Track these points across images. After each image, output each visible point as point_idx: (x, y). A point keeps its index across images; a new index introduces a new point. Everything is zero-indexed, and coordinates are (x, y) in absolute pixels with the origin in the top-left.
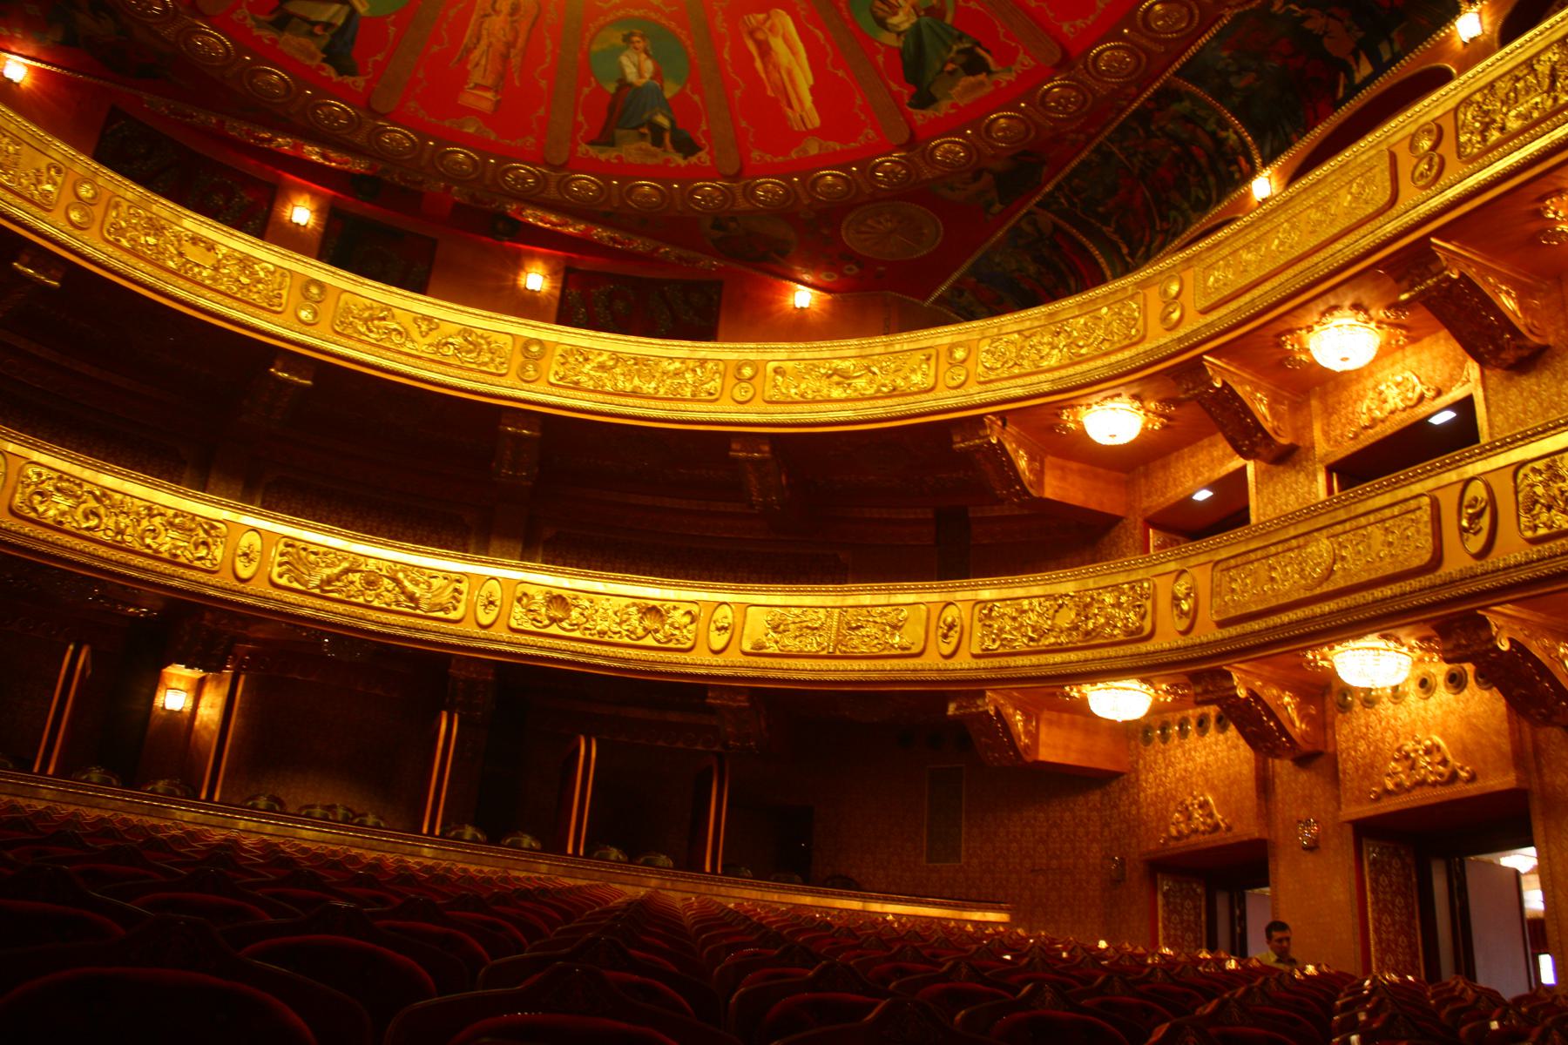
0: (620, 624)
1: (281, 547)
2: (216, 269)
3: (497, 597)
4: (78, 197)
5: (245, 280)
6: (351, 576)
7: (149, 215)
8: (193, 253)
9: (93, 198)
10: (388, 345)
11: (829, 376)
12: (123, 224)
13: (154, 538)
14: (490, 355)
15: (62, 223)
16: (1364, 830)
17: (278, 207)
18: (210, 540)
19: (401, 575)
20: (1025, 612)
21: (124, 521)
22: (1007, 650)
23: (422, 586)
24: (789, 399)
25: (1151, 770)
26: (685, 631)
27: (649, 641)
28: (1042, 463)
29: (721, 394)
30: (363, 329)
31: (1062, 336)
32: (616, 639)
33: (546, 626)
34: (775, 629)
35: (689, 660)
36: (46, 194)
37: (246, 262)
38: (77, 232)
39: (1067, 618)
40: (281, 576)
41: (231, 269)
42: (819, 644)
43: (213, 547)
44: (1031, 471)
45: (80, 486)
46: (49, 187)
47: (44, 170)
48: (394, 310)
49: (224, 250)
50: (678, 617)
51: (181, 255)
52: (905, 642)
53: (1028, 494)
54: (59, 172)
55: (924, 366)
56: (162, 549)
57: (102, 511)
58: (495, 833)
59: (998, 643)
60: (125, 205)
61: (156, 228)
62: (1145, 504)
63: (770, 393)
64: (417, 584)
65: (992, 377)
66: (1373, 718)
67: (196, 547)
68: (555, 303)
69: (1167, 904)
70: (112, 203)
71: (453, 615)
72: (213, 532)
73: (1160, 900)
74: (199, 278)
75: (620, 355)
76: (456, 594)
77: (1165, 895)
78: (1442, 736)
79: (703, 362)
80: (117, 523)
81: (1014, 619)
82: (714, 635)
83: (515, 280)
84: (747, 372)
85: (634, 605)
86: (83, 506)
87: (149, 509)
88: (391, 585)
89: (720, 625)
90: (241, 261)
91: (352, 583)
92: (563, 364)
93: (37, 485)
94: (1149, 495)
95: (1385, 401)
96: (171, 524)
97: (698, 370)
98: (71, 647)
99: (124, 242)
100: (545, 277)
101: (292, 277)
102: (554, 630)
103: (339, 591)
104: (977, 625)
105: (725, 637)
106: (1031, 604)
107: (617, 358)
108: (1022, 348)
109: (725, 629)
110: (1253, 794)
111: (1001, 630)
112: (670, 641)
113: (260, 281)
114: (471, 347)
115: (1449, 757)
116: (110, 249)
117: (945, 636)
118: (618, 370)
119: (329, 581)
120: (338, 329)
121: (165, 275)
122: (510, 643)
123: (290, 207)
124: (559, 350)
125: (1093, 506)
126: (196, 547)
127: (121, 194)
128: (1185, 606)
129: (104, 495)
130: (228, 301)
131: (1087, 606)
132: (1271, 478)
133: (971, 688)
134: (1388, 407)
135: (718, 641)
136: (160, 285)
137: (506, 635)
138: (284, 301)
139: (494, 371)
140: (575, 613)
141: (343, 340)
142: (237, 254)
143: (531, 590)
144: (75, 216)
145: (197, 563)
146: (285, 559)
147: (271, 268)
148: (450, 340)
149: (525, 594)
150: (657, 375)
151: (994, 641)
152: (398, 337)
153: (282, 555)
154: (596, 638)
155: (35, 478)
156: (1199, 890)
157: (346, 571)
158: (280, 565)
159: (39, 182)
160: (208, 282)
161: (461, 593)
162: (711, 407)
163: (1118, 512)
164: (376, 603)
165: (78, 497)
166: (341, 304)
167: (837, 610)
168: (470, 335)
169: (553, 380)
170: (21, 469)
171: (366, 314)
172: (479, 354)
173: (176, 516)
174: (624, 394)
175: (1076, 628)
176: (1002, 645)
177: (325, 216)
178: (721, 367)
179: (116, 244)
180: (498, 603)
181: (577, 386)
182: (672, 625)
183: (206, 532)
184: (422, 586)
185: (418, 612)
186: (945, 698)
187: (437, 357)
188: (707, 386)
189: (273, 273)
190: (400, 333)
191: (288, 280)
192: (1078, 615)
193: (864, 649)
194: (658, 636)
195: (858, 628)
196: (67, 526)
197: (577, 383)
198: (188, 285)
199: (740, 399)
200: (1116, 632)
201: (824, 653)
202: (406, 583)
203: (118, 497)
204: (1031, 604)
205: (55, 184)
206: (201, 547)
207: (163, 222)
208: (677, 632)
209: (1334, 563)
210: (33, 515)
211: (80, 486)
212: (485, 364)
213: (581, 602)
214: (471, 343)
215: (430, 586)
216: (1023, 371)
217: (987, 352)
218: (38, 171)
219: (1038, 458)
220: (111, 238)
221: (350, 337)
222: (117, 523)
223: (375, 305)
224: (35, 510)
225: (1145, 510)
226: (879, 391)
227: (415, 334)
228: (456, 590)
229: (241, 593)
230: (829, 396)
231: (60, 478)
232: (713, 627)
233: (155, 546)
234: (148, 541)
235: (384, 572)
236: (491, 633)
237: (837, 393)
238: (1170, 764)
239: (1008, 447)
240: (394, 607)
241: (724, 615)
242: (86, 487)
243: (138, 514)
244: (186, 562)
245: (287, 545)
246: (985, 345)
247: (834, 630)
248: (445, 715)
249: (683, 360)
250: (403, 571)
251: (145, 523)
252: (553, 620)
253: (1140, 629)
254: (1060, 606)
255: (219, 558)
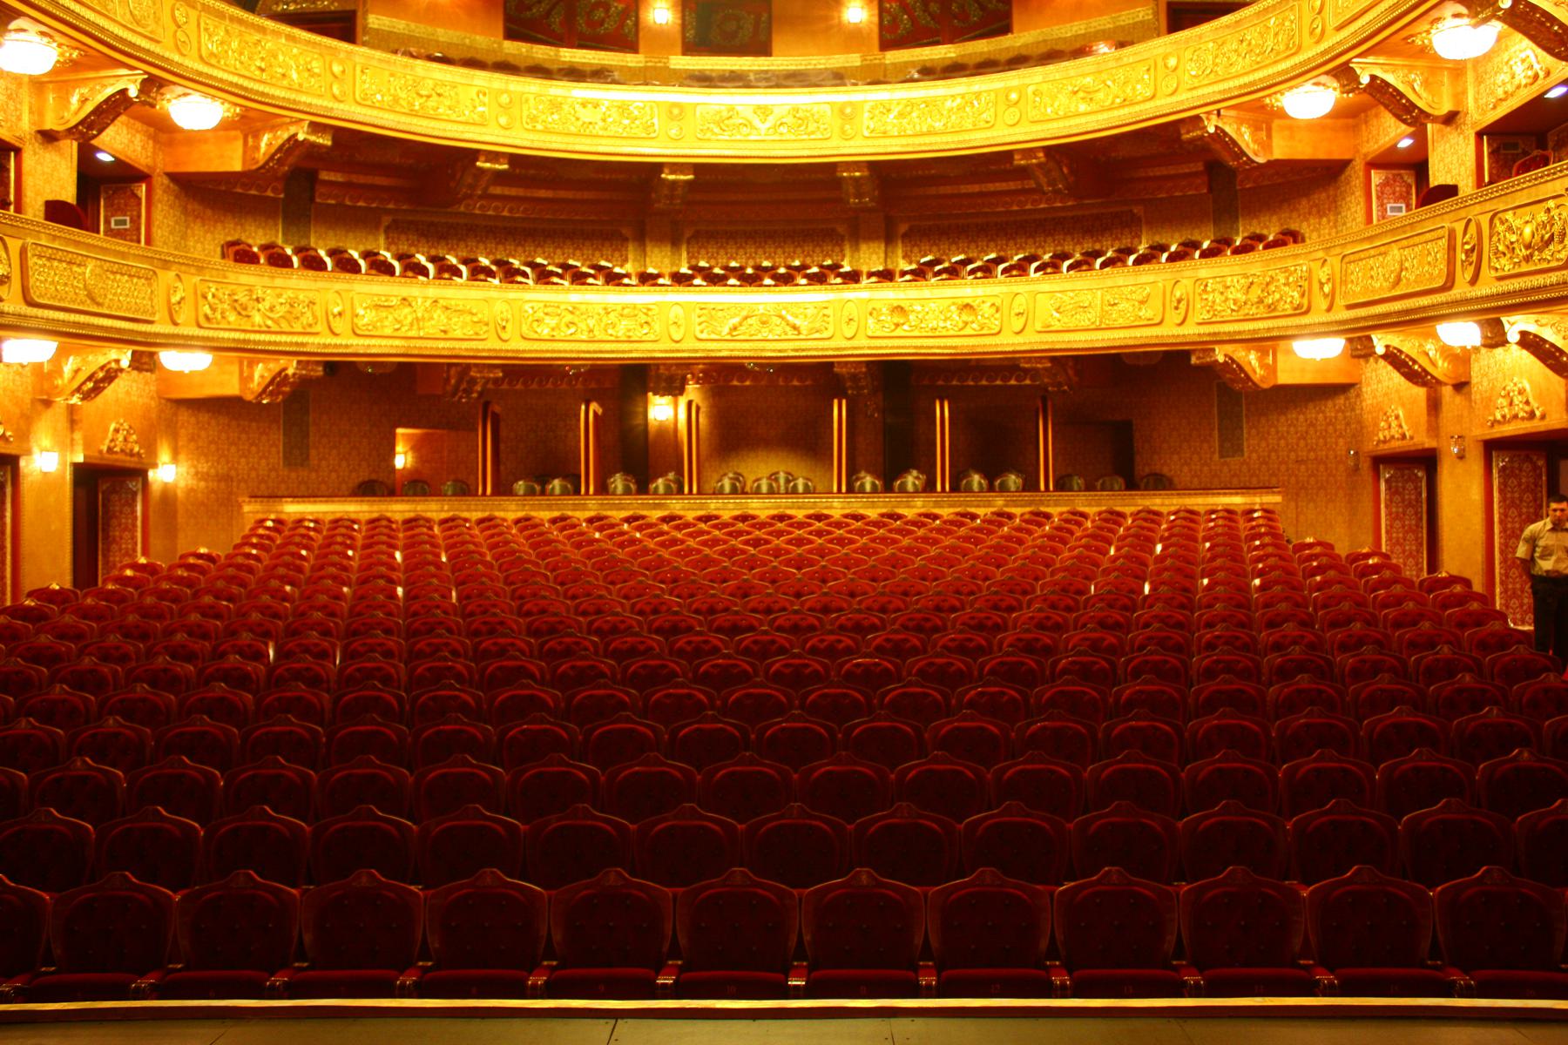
0: (945, 320)
1: (698, 312)
2: (604, 120)
3: (855, 315)
4: (500, 106)
5: (626, 122)
6: (750, 321)
7: (549, 98)
8: (587, 115)
9: (511, 102)
10: (738, 137)
11: (1075, 93)
12: (535, 112)
13: (614, 328)
14: (815, 125)
15: (498, 131)
16: (1492, 447)
17: (642, 15)
18: (649, 319)
19: (784, 313)
20: (1229, 287)
21: (591, 322)
22: (1218, 319)
23: (800, 316)
24: (1047, 118)
25: (1368, 385)
26: (992, 319)
27: (968, 331)
28: (1269, 131)
29: (995, 120)
30: (717, 130)
31: (1244, 44)
32: (944, 333)
33: (893, 331)
34: (1057, 310)
35: (998, 342)
36: (482, 115)
37: (623, 108)
38: (507, 133)
39: (1256, 292)
40: (702, 332)
41: (615, 114)
42: (1089, 320)
43: (652, 324)
44: (1255, 141)
45: (558, 307)
46: (480, 109)
47: (476, 98)
48: (737, 108)
49: (607, 104)
50: (987, 310)
51: (578, 119)
52: (1149, 314)
53: (1253, 161)
54: (485, 94)
55: (1146, 77)
56: (619, 334)
57: (576, 320)
58: (889, 481)
59: (1212, 313)
60: (531, 97)
61: (556, 106)
62: (1364, 150)
63: (1033, 114)
64: (797, 317)
65: (1196, 85)
66: (1492, 361)
67: (642, 327)
68: (876, 29)
69: (1389, 488)
70: (523, 100)
71: (826, 334)
72: (650, 313)
73: (1383, 486)
74: (594, 132)
75: (914, 101)
76: (825, 318)
77: (1387, 481)
78: (1531, 382)
79: (978, 95)
80: (587, 325)
81: (1222, 293)
82: (1014, 319)
83: (839, 17)
84: (1014, 96)
85: (954, 304)
86: (564, 320)
87: (605, 309)
88: (778, 321)
89: (1017, 311)
90: (620, 107)
91: (751, 325)
92: (872, 118)
93: (532, 315)
94: (1368, 142)
95: (1513, 77)
96: (622, 315)
97: (975, 102)
98: (583, 407)
99: (539, 127)
100: (862, 8)
101: (658, 107)
102: (899, 332)
103: (744, 334)
104: (1198, 298)
105: (1022, 320)
106: (1232, 280)
107: (911, 104)
108: (1216, 57)
109: (1022, 314)
110: (1425, 411)
111: (1214, 302)
112: (982, 329)
113: (636, 119)
114: (800, 122)
115: (1531, 400)
116: (531, 136)
117: (1176, 308)
118: (915, 114)
119: (735, 328)
120: (699, 136)
121: (571, 139)
122: (869, 348)
123: (651, 11)
124: (867, 107)
125: (1321, 155)
126: (642, 327)
127: (527, 90)
128: (1327, 289)
129: (574, 308)
130: (618, 142)
131: (1268, 284)
132: (1443, 136)
133: (1207, 346)
134: (1516, 82)
135: (1018, 324)
136: (570, 148)
137: (866, 342)
138: (656, 127)
139: (820, 137)
140: (912, 317)
141: (706, 144)
142: (615, 104)
143: (877, 306)
144: (503, 120)
145: (644, 338)
146: (702, 319)
147: (642, 105)
148: (784, 120)
149: (874, 309)
150: (945, 112)
151: (1208, 312)
152: (745, 129)
153: (699, 317)
154: (930, 334)
155: (531, 311)
156: (1420, 474)
157: (746, 318)
158: (700, 324)
159: (475, 107)
160: (601, 133)
161: (829, 317)
162: (989, 134)
163: (1346, 157)
164: (770, 337)
165: (559, 315)
166: (698, 114)
167: (1099, 292)
168: (797, 112)
169: (866, 133)
170: (520, 310)
171: (718, 118)
172: (807, 126)
173: (623, 309)
174: (922, 134)
175: (1261, 301)
176: (1215, 315)
177: (680, 8)
178: (993, 96)
179: (534, 130)
180: (856, 319)
181: (885, 135)
182: (982, 316)
183: (646, 314)
184: (800, 316)
185: (801, 337)
186: (1187, 354)
187: (777, 137)
188: (984, 116)
189: (643, 108)
190: (745, 125)
191: (656, 110)
192: (1263, 291)
193: (1121, 321)
194: (974, 326)
195: (1115, 304)
196: (557, 338)
197: (885, 133)
198: (589, 141)
199: (1009, 123)
200: (1287, 306)
201: (1093, 327)
202: (789, 318)
203: (583, 307)
204: (1232, 280)
205: (484, 104)
206: (645, 326)
207: (559, 99)
208: (987, 321)
209: (1402, 270)
210: (536, 336)
211: (558, 307)
212: (813, 133)
213: (915, 308)
214: (799, 119)
215: (806, 316)
216: (1220, 78)
217: (1191, 59)
218: (472, 100)
219: (1264, 126)
220: (529, 127)
221: (709, 140)
222: (587, 325)
223: (722, 108)
224: (536, 332)
225: (1365, 155)
226: (1113, 103)
227: (756, 121)
228: (824, 315)
229: (678, 351)
230: (1077, 111)
231: (545, 306)
232: (1013, 313)
233: (614, 334)
234: (610, 331)
235: (772, 313)
236: (854, 343)
237: (1083, 107)
238: (1379, 382)
239: (1228, 129)
240: (783, 337)
241: (1020, 304)
242: (563, 307)
243: (599, 314)
244: (637, 339)
245: (702, 309)
246: (1188, 54)
247: (1099, 309)
248: (836, 402)
249: (963, 96)
250: (785, 308)
251: (605, 319)
252: (897, 325)
253: (1299, 306)
254: (1252, 283)
255: (658, 331)
